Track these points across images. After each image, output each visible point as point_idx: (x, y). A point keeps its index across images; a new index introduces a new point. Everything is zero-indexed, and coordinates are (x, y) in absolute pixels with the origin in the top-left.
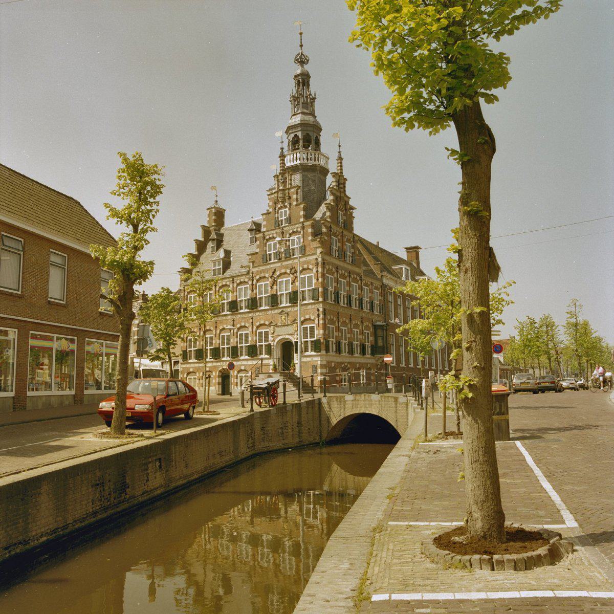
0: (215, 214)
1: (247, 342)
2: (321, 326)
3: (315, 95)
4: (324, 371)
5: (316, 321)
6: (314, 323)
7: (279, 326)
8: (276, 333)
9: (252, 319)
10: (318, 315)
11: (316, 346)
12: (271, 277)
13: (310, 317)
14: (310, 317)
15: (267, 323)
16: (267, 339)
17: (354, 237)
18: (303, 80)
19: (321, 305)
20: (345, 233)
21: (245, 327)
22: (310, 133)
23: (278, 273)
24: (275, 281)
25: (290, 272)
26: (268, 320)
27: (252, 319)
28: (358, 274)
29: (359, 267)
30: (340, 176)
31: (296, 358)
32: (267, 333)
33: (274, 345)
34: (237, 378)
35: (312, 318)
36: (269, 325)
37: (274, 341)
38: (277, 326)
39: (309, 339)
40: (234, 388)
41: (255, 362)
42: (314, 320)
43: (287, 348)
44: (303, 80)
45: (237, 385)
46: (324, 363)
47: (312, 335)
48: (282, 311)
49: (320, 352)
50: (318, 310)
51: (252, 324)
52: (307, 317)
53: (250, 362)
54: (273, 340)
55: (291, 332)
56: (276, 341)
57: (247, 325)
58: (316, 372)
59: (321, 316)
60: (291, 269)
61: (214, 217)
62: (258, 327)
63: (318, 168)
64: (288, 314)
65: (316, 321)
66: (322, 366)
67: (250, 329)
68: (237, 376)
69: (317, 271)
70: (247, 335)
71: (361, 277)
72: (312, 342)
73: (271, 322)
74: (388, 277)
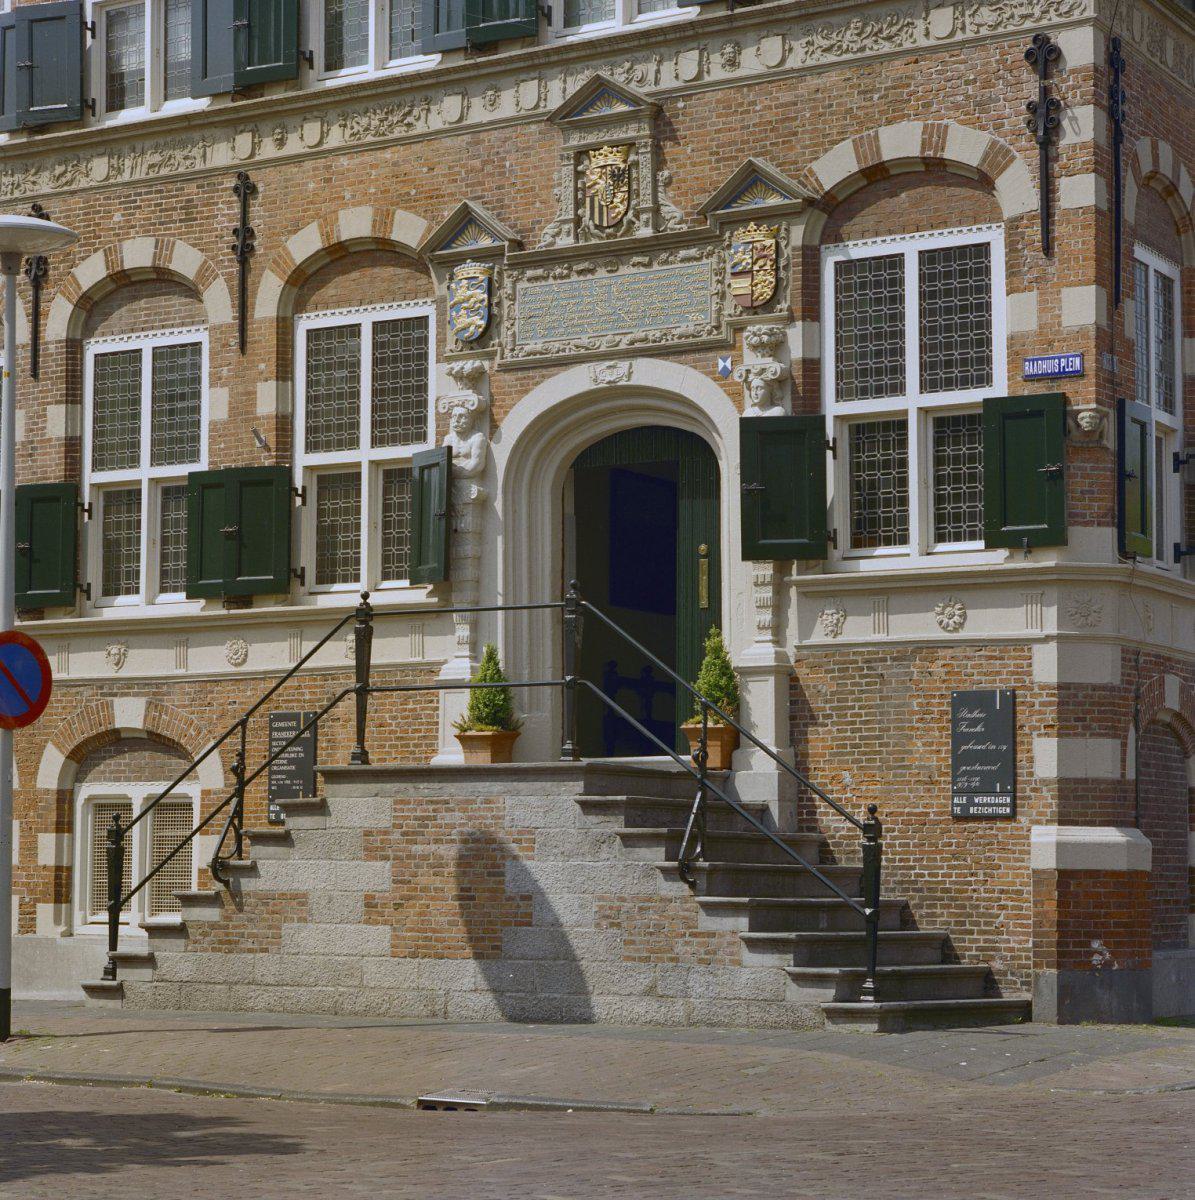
1: (176, 441)
2: (1078, 241)
4: (1104, 759)
5: (1017, 190)
6: (993, 215)
7: (550, 259)
8: (521, 337)
9: (246, 190)
10: (1046, 118)
11: (1014, 473)
13: (935, 136)
14: (935, 136)
15: (410, 230)
16: (402, 411)
21: (160, 280)
26: (424, 201)
27: (246, 190)
31: (749, 619)
32: (402, 347)
33: (484, 473)
34: (64, 825)
35: (965, 146)
36: (437, 257)
37: (487, 429)
38: (521, 257)
39: (912, 400)
40: (29, 926)
41: (271, 655)
42: (983, 181)
43: (631, 503)
45: (60, 889)
46: (1103, 669)
47: (958, 349)
48: (599, 90)
49: (1055, 539)
50: (1044, 56)
51: (244, 251)
52: (900, 141)
53: (210, 659)
54: (484, 419)
55: (693, 323)
56: (516, 422)
57: (185, 261)
58: (1007, 773)
59: (1081, 125)
62: (305, 283)
64: (659, 116)
65: (1017, 190)
66: (1077, 709)
67: (218, 301)
68: (65, 798)
70: (177, 363)
72: (946, 426)
73: (465, 220)
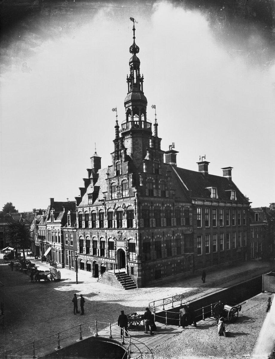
3: (143, 76)
12: (114, 209)
18: (135, 64)
19: (137, 231)
23: (117, 206)
25: (123, 207)
44: (135, 64)
50: (136, 234)
60: (123, 205)
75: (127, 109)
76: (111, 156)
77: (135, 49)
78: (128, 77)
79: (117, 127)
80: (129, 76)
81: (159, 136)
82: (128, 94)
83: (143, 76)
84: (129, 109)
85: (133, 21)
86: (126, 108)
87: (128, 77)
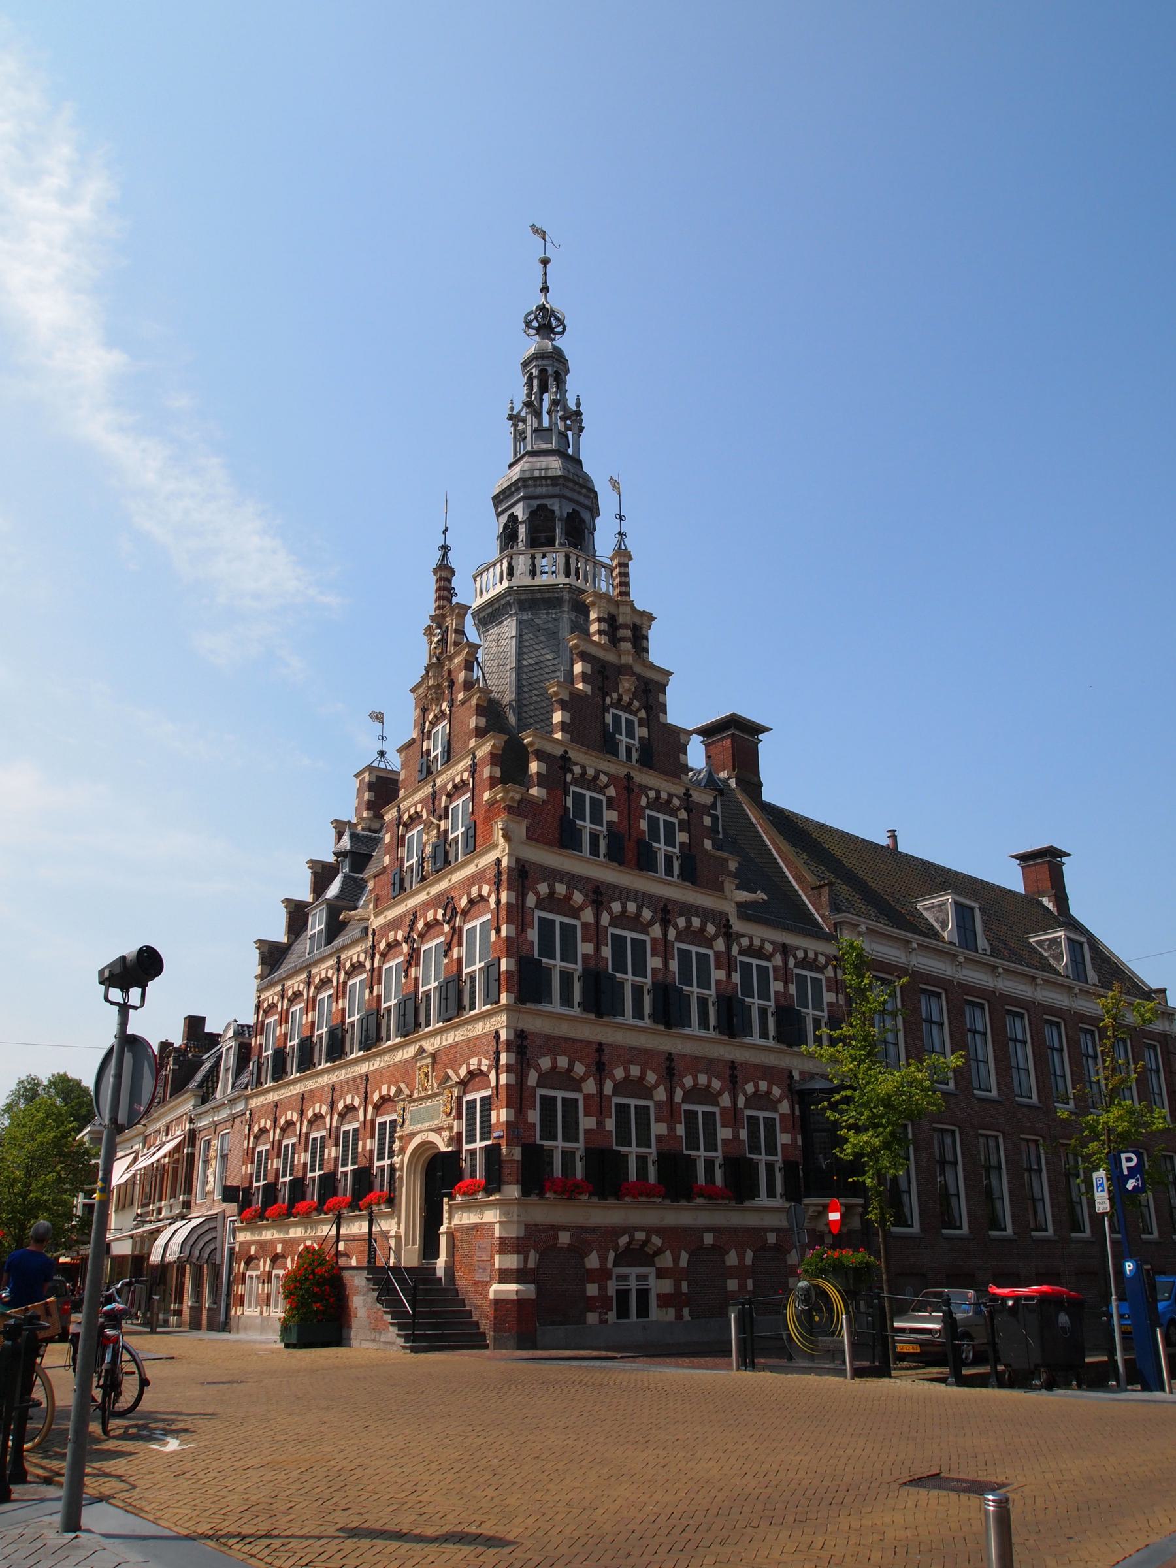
0: (371, 787)
3: (578, 405)
17: (687, 795)
18: (548, 371)
20: (642, 777)
22: (554, 505)
24: (414, 950)
28: (707, 915)
29: (718, 888)
30: (617, 604)
44: (548, 371)
61: (366, 796)
63: (566, 596)
69: (498, 902)
71: (728, 926)
74: (863, 928)
75: (504, 519)
76: (412, 696)
77: (546, 323)
78: (512, 409)
79: (444, 573)
80: (518, 406)
81: (641, 598)
82: (511, 466)
83: (578, 405)
84: (513, 518)
85: (544, 239)
86: (498, 515)
87: (512, 409)
